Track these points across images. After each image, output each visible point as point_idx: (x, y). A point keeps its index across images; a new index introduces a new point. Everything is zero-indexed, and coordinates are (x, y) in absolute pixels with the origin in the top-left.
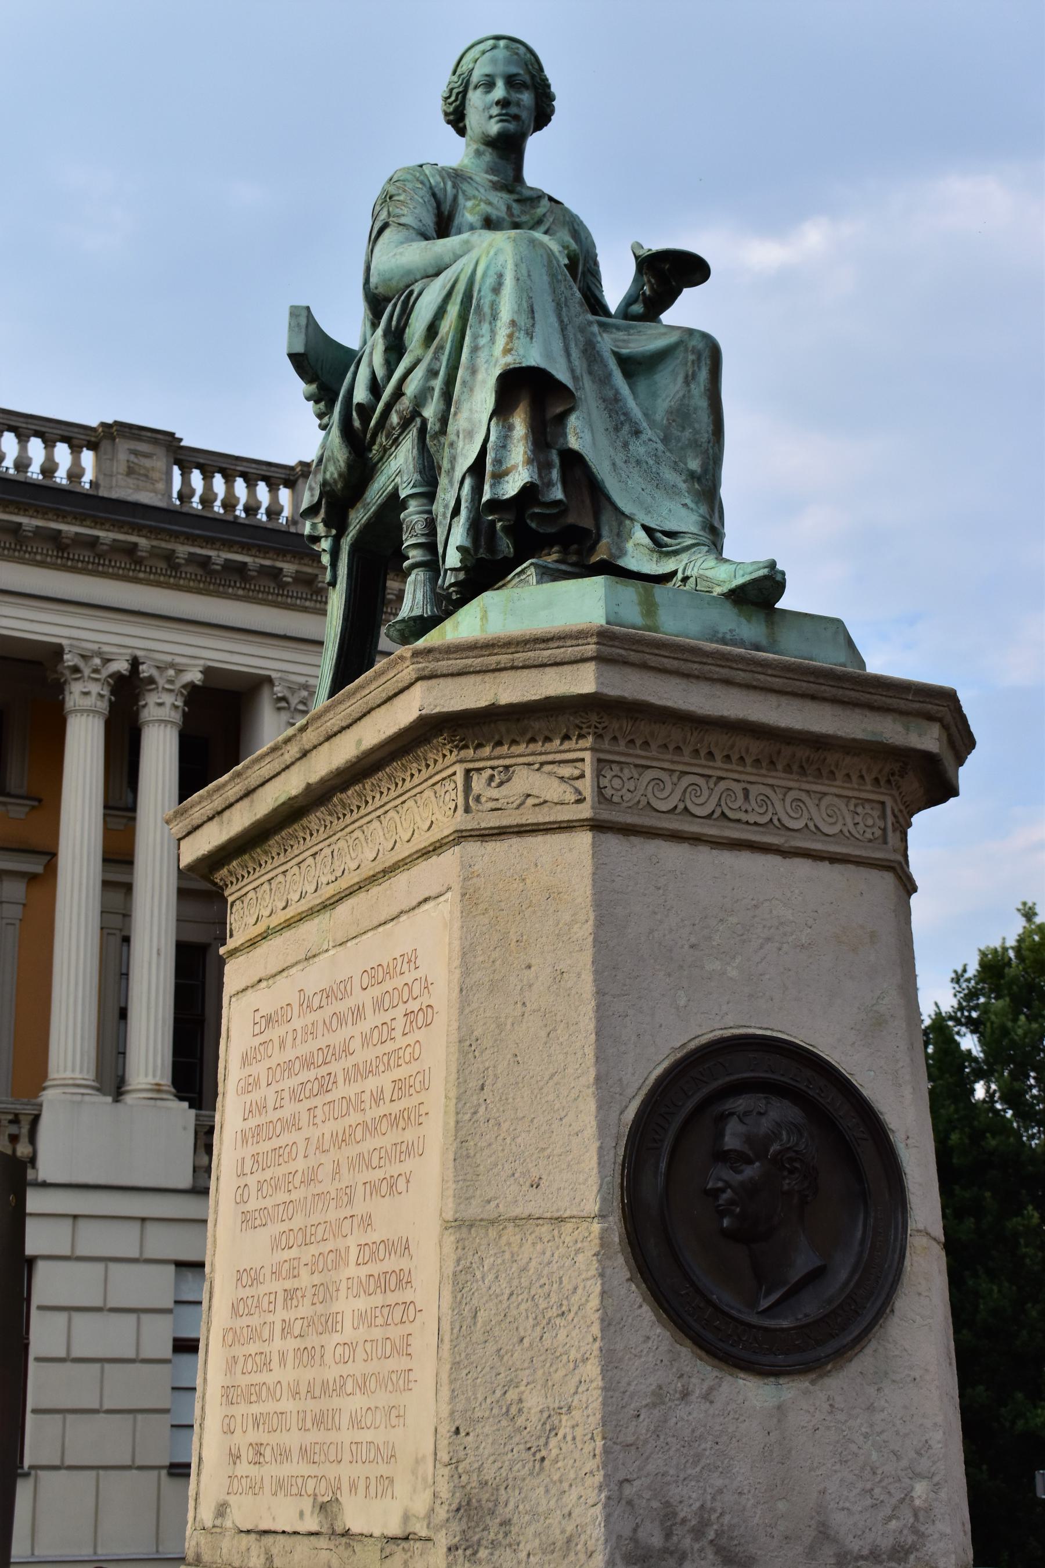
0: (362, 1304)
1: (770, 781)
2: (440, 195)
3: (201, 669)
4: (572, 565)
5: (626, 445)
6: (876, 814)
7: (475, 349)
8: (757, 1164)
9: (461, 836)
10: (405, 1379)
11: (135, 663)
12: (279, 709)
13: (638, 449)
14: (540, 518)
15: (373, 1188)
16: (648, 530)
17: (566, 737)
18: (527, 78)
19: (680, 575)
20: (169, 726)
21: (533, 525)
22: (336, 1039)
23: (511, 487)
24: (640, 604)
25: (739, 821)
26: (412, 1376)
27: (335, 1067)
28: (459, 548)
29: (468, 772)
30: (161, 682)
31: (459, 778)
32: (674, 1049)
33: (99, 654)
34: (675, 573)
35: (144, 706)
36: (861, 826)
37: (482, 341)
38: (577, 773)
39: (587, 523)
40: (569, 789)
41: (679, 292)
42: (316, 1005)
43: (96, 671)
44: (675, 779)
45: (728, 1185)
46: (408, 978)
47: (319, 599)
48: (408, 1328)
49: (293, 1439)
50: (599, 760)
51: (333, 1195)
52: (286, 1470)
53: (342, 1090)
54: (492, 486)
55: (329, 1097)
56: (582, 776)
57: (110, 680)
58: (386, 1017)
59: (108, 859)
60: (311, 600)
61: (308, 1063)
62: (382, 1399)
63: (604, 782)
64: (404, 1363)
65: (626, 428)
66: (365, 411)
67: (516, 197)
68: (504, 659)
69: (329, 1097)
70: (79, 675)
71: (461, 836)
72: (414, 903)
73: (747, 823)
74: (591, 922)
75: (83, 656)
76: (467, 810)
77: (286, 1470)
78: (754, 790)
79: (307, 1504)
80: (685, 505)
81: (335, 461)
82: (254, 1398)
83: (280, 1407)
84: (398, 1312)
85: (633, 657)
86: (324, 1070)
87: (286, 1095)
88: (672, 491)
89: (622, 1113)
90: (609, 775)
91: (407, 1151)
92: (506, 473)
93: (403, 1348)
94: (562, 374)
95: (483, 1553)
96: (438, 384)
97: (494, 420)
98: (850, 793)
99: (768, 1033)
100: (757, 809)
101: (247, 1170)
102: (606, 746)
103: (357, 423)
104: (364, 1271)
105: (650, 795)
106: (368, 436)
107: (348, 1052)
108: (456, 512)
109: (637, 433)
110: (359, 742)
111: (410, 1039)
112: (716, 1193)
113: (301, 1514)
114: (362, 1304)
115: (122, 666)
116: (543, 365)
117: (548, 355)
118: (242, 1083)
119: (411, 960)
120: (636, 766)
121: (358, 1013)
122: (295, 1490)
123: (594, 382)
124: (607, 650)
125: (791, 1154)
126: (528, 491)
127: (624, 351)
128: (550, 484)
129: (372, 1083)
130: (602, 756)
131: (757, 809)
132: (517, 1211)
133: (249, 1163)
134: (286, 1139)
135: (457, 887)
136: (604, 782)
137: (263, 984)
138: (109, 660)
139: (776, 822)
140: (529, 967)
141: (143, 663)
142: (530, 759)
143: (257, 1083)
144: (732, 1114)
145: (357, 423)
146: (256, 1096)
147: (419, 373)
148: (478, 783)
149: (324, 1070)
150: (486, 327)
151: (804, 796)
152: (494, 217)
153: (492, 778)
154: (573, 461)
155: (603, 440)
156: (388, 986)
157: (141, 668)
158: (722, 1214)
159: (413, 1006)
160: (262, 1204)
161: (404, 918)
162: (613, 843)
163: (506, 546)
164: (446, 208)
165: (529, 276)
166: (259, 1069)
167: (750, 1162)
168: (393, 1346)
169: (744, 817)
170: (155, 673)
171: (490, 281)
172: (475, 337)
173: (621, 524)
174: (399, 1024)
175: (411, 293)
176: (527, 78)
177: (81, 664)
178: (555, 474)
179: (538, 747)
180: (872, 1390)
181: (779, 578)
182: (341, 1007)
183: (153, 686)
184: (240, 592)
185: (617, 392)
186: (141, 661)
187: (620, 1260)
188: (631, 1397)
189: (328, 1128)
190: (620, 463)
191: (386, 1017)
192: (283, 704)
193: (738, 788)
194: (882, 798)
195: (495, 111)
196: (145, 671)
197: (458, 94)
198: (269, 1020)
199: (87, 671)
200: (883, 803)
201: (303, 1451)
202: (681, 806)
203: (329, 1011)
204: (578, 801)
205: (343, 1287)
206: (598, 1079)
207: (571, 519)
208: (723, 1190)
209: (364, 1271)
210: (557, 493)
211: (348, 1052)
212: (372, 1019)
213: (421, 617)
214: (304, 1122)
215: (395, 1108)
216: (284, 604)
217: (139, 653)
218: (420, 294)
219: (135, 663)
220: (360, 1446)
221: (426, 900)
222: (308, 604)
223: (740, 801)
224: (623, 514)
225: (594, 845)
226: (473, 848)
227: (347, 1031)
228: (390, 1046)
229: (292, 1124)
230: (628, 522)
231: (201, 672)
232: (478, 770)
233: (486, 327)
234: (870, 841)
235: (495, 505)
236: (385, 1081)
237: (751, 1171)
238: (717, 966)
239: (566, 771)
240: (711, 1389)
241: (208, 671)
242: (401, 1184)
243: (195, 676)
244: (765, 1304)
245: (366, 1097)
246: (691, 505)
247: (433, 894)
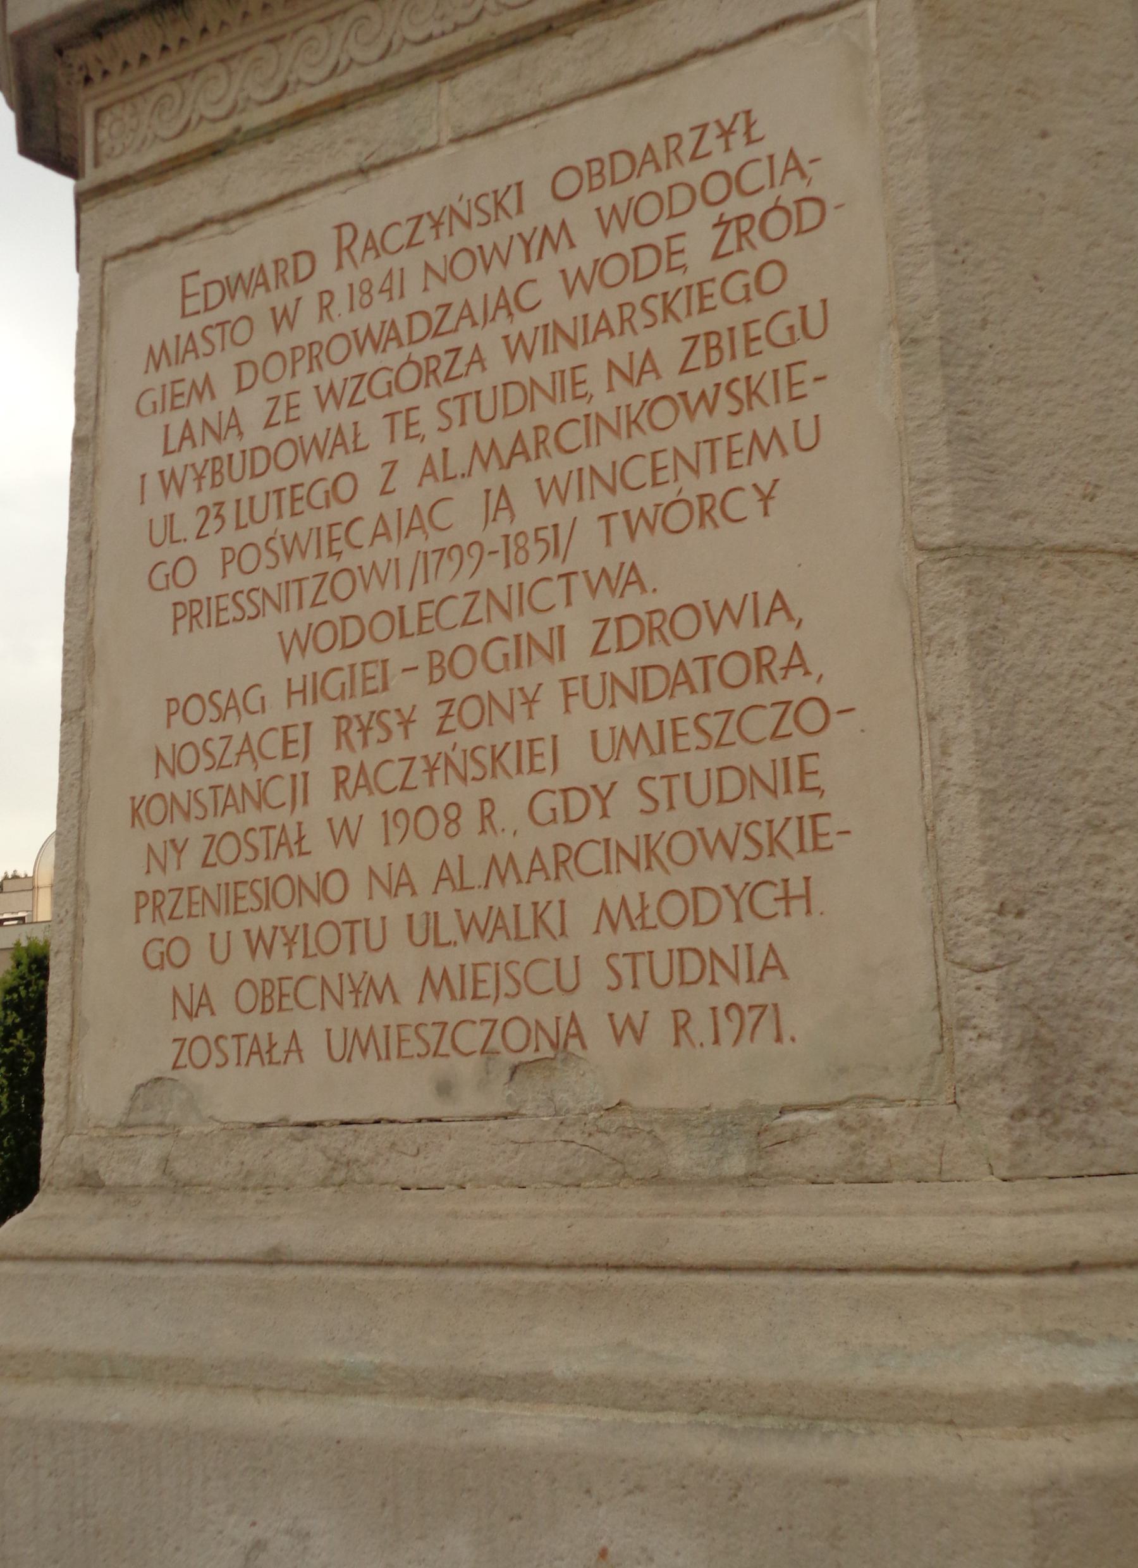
64: (794, 804)
79: (466, 1069)
95: (1072, 1121)
104: (621, 665)
111: (748, 260)
113: (444, 1088)
132: (1063, 539)
140: (1044, 135)
198: (231, 287)
209: (621, 665)
220: (643, 963)
228: (665, 282)
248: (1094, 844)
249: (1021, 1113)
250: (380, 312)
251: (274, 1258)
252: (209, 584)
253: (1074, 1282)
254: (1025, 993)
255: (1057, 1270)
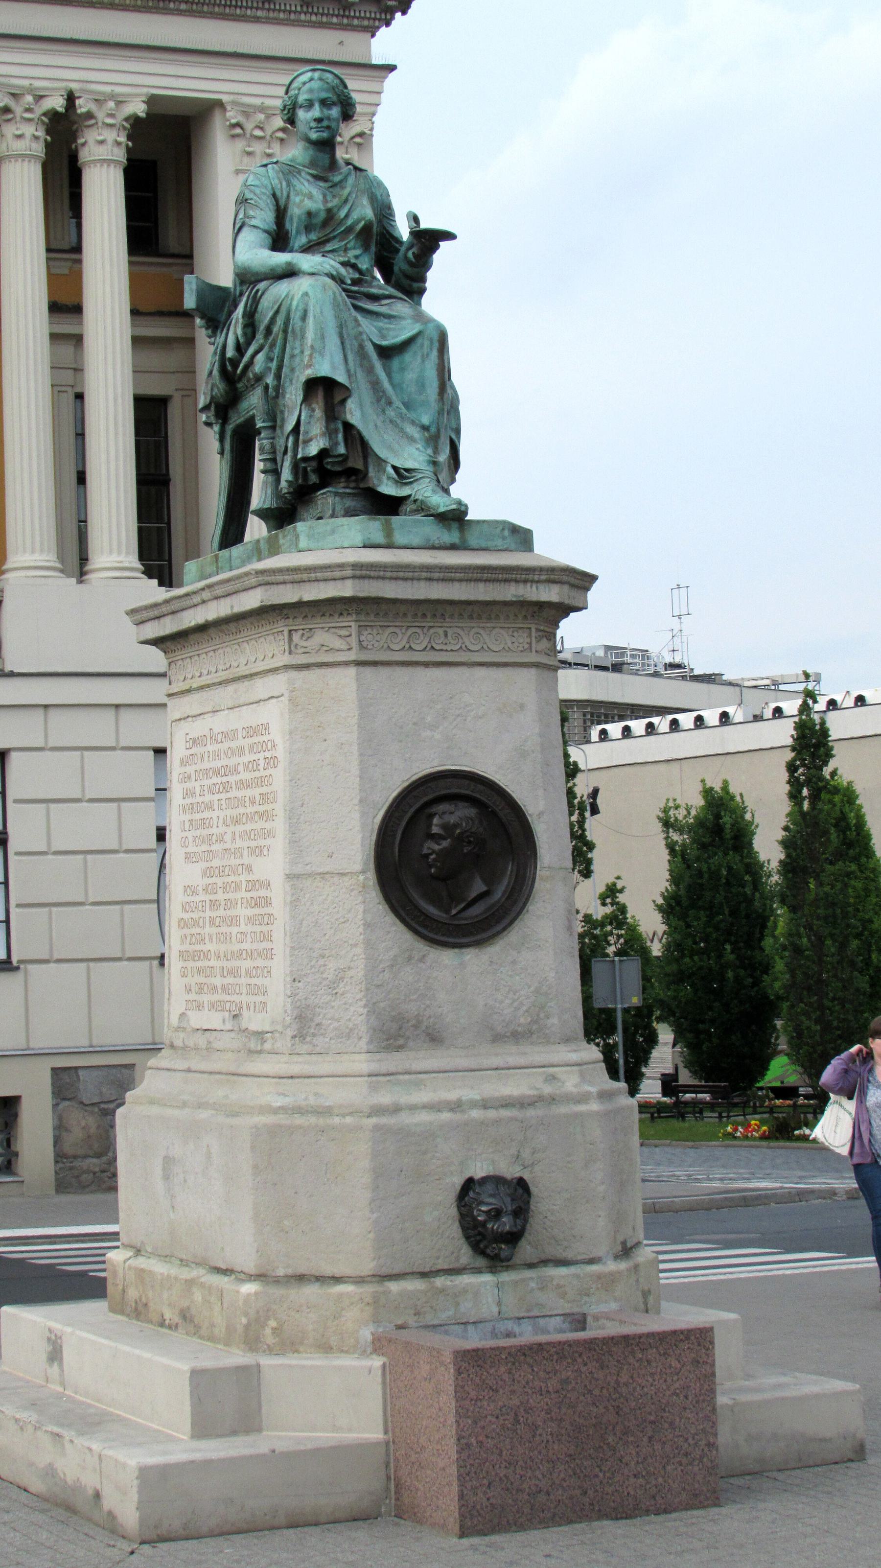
0: (250, 912)
1: (460, 625)
2: (278, 194)
3: (144, 99)
4: (353, 488)
5: (383, 411)
6: (525, 635)
7: (292, 356)
8: (449, 840)
9: (287, 667)
10: (268, 955)
11: (71, 98)
12: (233, 136)
13: (391, 413)
14: (333, 463)
15: (252, 851)
16: (395, 468)
17: (341, 614)
18: (335, 98)
19: (412, 498)
20: (112, 166)
21: (329, 467)
22: (232, 762)
23: (313, 450)
24: (383, 530)
25: (442, 650)
26: (274, 952)
27: (232, 779)
28: (287, 481)
29: (290, 631)
30: (101, 115)
31: (286, 633)
32: (403, 781)
33: (30, 90)
34: (410, 496)
35: (84, 144)
36: (516, 644)
37: (297, 352)
38: (347, 633)
39: (359, 465)
40: (344, 643)
41: (437, 247)
42: (219, 740)
43: (29, 110)
44: (404, 631)
45: (434, 852)
46: (265, 738)
47: (272, 6)
48: (270, 927)
49: (218, 981)
50: (360, 626)
51: (233, 850)
52: (216, 997)
53: (234, 793)
54: (303, 449)
55: (229, 795)
56: (350, 635)
57: (43, 118)
58: (256, 757)
59: (55, 308)
60: (263, 9)
61: (217, 773)
62: (260, 962)
63: (363, 638)
65: (383, 401)
66: (235, 363)
67: (330, 184)
68: (305, 576)
69: (229, 795)
70: (10, 116)
71: (287, 667)
72: (266, 697)
73: (447, 650)
74: (356, 717)
75: (14, 95)
76: (290, 653)
77: (216, 997)
78: (450, 632)
80: (417, 449)
81: (218, 388)
82: (197, 958)
83: (211, 963)
84: (266, 918)
85: (372, 574)
86: (225, 779)
87: (206, 788)
88: (412, 439)
89: (374, 817)
90: (365, 633)
91: (268, 834)
92: (311, 440)
93: (267, 937)
94: (341, 378)
95: (308, 1039)
96: (274, 365)
97: (303, 406)
98: (509, 625)
99: (458, 768)
100: (452, 641)
101: (187, 829)
102: (362, 617)
103: (229, 368)
104: (249, 895)
105: (389, 642)
106: (238, 371)
107: (236, 771)
108: (285, 452)
109: (390, 403)
110: (232, 607)
111: (267, 772)
112: (427, 856)
113: (224, 1021)
114: (250, 912)
115: (57, 103)
116: (329, 375)
117: (334, 367)
118: (181, 776)
119: (266, 727)
120: (381, 626)
121: (241, 750)
122: (220, 1008)
123: (363, 371)
124: (358, 573)
125: (468, 834)
126: (323, 453)
127: (384, 343)
128: (337, 444)
129: (249, 793)
130: (362, 624)
131: (452, 641)
132: (321, 870)
133: (187, 824)
134: (206, 814)
135: (287, 695)
136: (363, 638)
137: (190, 719)
138: (42, 97)
139: (463, 646)
140: (325, 740)
141: (79, 97)
142: (323, 625)
143: (189, 777)
144: (435, 814)
145: (229, 368)
146: (189, 785)
147: (260, 357)
148: (296, 637)
149: (225, 779)
150: (298, 343)
151: (482, 632)
152: (313, 210)
153: (303, 634)
154: (348, 427)
155: (369, 410)
156: (256, 739)
157: (78, 102)
158: (430, 866)
159: (268, 755)
160: (195, 849)
161: (262, 703)
162: (368, 671)
163: (313, 478)
164: (282, 203)
165: (321, 313)
166: (190, 769)
167: (445, 839)
168: (264, 935)
169: (444, 648)
170: (92, 107)
171: (299, 314)
172: (293, 348)
173: (379, 465)
174: (262, 763)
175: (258, 291)
176: (335, 98)
177: (12, 104)
178: (340, 436)
179: (327, 619)
180: (515, 953)
181: (463, 508)
182: (234, 744)
183: (92, 122)
184: (183, 6)
185: (378, 378)
186: (77, 95)
187: (374, 894)
188: (381, 961)
189: (229, 812)
190: (379, 423)
191: (256, 757)
192: (238, 131)
193: (441, 631)
194: (529, 626)
195: (313, 124)
196: (83, 106)
197: (289, 110)
198: (195, 742)
199: (18, 110)
200: (530, 628)
201: (223, 988)
202: (407, 646)
203: (226, 745)
204: (349, 649)
205: (239, 902)
206: (361, 801)
207: (350, 464)
208: (431, 854)
209: (249, 895)
210: (342, 450)
211: (236, 771)
212: (248, 757)
213: (270, 509)
214: (216, 807)
215: (261, 809)
216: (232, 15)
217: (74, 86)
218: (263, 294)
219: (71, 98)
221: (272, 697)
222: (259, 13)
223: (442, 639)
224: (379, 458)
225: (357, 674)
226: (293, 674)
227: (234, 760)
228: (257, 774)
229: (210, 807)
230: (383, 464)
231: (144, 102)
232: (296, 630)
233: (298, 343)
234: (521, 651)
235: (305, 459)
236: (256, 792)
237: (445, 844)
238: (428, 733)
239: (344, 632)
240: (424, 956)
241: (152, 100)
242: (265, 852)
243: (139, 108)
244: (454, 912)
245: (247, 799)
246: (421, 448)
247: (276, 694)
248: (321, 962)
249: (294, 1037)
250: (217, 764)
251: (189, 1070)
252: (192, 849)
253: (290, 1081)
254: (298, 1004)
255: (288, 1077)
